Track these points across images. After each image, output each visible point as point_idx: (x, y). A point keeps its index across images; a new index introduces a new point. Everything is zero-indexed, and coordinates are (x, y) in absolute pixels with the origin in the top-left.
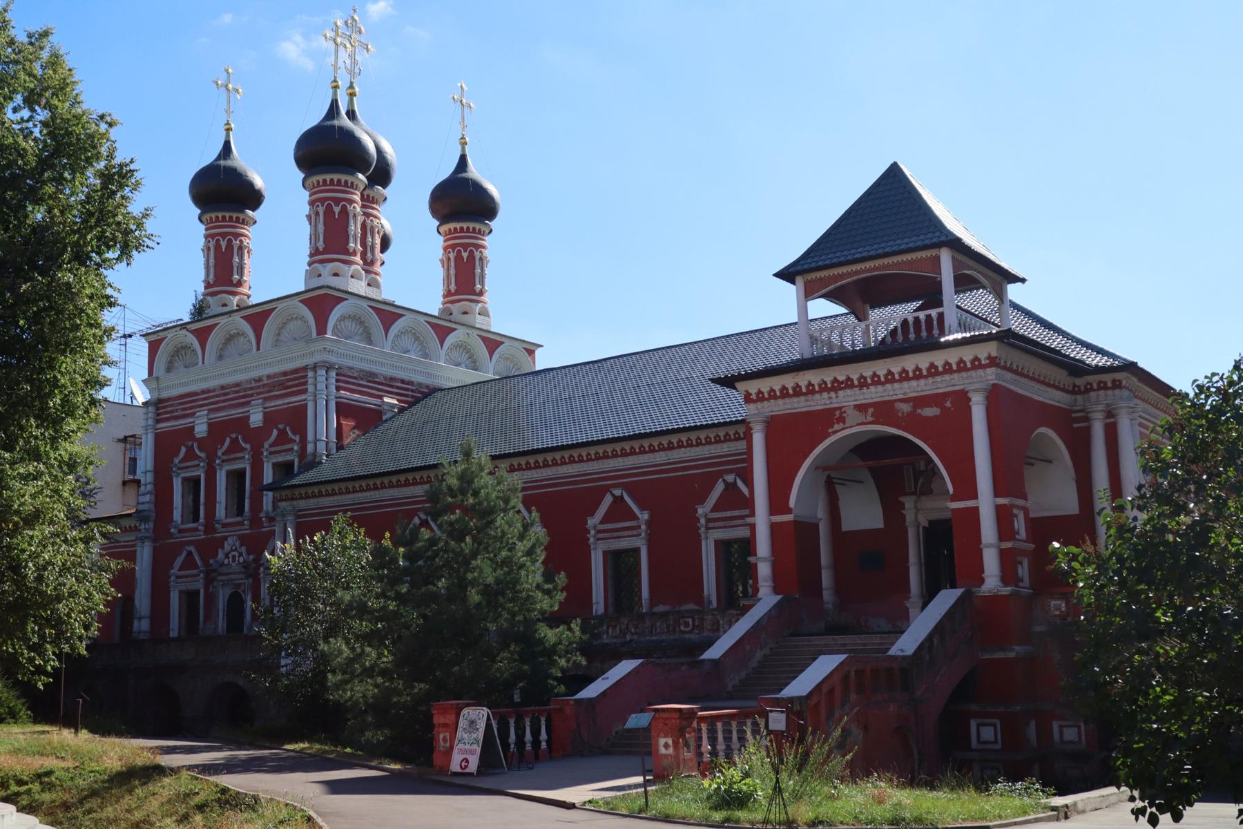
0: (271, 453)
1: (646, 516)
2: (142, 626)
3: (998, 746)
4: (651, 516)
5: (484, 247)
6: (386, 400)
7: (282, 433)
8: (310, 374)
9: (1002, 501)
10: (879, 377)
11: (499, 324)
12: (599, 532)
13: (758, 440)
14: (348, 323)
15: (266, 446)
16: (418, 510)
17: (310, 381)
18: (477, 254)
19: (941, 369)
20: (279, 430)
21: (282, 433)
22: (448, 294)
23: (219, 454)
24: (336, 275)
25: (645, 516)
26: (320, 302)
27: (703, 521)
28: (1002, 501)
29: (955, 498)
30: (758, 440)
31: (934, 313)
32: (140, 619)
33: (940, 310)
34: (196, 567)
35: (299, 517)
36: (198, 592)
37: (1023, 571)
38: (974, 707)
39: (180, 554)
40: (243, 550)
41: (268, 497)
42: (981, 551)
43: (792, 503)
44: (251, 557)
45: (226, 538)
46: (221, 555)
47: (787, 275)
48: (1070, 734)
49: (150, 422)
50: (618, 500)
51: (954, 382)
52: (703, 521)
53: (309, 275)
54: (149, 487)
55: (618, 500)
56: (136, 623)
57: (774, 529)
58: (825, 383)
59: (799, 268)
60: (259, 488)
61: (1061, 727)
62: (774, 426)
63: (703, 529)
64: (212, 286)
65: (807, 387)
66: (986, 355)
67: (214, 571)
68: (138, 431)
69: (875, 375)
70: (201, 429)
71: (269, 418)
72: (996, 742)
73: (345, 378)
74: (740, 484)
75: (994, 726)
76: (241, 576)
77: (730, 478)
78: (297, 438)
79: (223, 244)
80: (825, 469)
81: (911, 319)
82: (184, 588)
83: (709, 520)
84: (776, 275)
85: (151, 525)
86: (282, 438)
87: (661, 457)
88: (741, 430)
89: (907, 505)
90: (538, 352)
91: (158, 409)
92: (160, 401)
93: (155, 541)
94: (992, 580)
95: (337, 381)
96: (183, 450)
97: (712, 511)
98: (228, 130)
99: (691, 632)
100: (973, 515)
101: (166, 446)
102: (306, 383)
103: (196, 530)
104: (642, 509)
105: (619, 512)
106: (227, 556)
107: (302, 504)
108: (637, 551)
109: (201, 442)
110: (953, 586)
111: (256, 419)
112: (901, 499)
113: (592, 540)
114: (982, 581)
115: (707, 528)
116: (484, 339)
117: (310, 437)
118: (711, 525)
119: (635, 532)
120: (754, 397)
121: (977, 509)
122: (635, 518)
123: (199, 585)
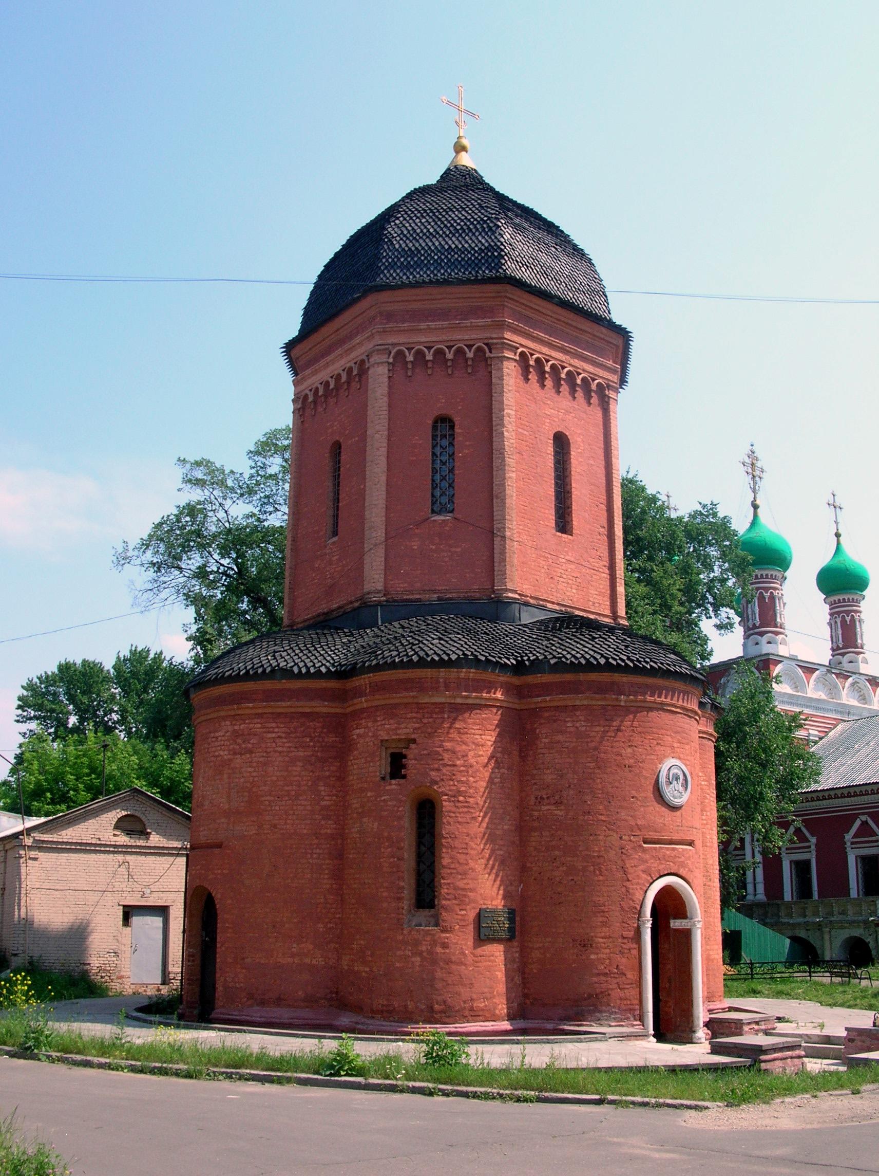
5: (860, 612)
16: (859, 814)
18: (856, 617)
22: (835, 650)
53: (745, 646)
116: (868, 680)
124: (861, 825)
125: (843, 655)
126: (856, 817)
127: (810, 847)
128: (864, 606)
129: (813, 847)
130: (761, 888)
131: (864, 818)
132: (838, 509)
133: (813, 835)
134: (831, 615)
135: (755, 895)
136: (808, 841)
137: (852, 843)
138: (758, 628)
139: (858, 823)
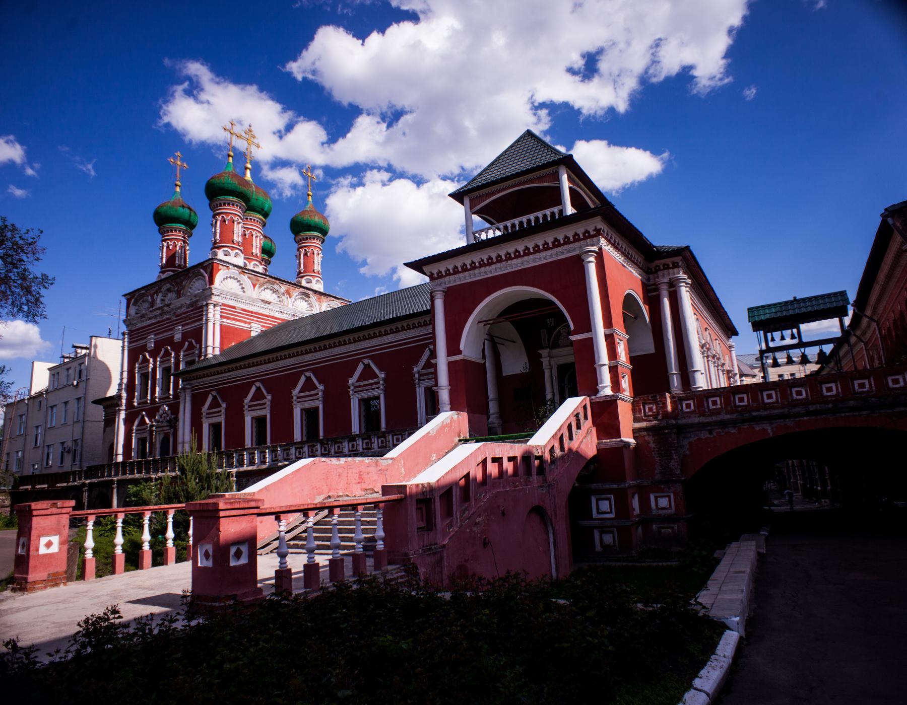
1: (383, 376)
3: (612, 516)
4: (386, 375)
7: (190, 343)
8: (205, 308)
9: (609, 331)
12: (356, 387)
19: (562, 242)
21: (190, 343)
25: (382, 375)
27: (417, 376)
29: (576, 332)
31: (556, 210)
33: (559, 207)
38: (594, 486)
39: (137, 417)
43: (462, 347)
48: (663, 502)
50: (367, 367)
52: (417, 376)
55: (367, 367)
57: (450, 364)
58: (482, 260)
61: (656, 498)
62: (450, 295)
65: (471, 265)
69: (517, 251)
71: (185, 336)
72: (611, 512)
73: (228, 311)
75: (609, 499)
78: (198, 346)
83: (420, 375)
84: (450, 195)
86: (191, 346)
87: (391, 338)
102: (202, 315)
104: (381, 370)
105: (368, 373)
108: (378, 398)
110: (576, 395)
111: (178, 337)
112: (540, 352)
114: (597, 391)
115: (420, 380)
118: (422, 378)
119: (377, 386)
120: (436, 275)
122: (376, 376)
123: (147, 435)
125: (302, 277)
126: (252, 383)
129: (223, 411)
133: (224, 401)
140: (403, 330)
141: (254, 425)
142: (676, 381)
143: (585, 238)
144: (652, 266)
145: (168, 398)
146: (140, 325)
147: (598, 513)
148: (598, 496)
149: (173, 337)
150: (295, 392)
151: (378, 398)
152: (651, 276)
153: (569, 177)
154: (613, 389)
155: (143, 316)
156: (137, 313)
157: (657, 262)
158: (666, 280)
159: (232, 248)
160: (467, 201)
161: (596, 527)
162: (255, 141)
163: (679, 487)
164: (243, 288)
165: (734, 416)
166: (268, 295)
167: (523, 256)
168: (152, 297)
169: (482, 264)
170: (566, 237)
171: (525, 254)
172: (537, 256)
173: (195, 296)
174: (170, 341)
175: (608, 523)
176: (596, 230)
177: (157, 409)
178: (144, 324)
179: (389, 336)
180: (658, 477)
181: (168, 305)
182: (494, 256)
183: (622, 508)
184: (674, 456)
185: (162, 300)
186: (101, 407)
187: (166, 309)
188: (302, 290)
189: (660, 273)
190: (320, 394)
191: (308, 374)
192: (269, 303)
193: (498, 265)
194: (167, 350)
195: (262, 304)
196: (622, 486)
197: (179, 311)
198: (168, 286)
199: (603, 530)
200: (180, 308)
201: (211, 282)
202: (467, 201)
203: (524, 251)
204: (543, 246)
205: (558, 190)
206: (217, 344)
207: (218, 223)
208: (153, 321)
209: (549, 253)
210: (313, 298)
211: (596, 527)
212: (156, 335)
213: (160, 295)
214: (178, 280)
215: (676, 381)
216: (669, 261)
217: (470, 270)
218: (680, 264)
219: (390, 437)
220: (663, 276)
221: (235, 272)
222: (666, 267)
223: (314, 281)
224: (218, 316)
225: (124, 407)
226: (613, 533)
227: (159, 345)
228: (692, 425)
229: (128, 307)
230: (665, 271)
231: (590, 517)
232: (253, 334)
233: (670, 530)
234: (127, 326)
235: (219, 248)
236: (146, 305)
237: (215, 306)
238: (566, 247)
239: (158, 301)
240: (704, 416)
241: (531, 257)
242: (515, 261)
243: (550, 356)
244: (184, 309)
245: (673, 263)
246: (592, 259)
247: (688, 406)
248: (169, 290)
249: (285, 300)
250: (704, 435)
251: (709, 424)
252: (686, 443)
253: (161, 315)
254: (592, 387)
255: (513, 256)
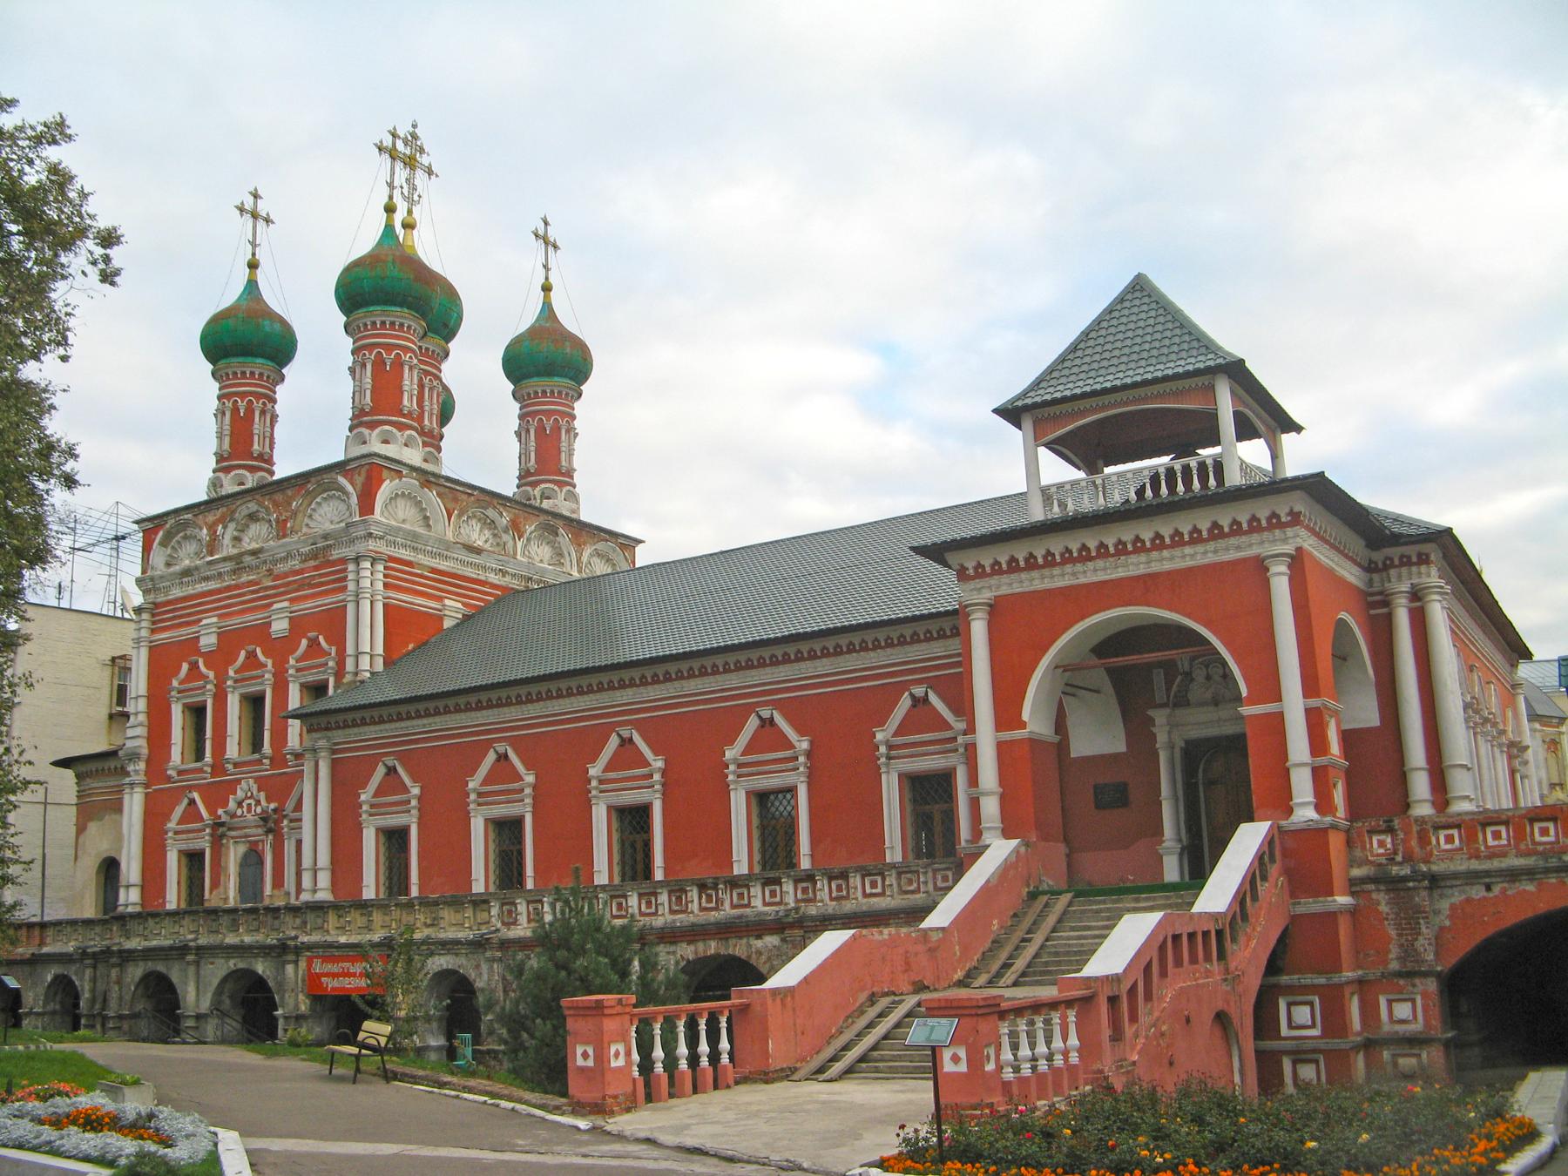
0: (298, 670)
1: (805, 745)
2: (130, 898)
3: (1316, 1032)
6: (447, 602)
7: (314, 643)
8: (351, 567)
9: (1314, 702)
10: (1143, 542)
11: (586, 516)
12: (740, 766)
13: (979, 629)
14: (401, 503)
15: (292, 662)
17: (351, 576)
18: (563, 423)
19: (1226, 530)
20: (309, 640)
21: (314, 643)
22: (524, 476)
23: (231, 673)
24: (386, 442)
26: (363, 474)
27: (883, 749)
28: (1314, 702)
29: (1252, 701)
30: (979, 629)
32: (128, 887)
34: (201, 819)
35: (334, 752)
36: (201, 854)
37: (1339, 796)
38: (1285, 979)
39: (178, 802)
40: (262, 794)
41: (294, 726)
42: (1287, 773)
43: (1025, 716)
44: (272, 806)
45: (239, 781)
46: (232, 805)
47: (1011, 413)
49: (144, 633)
51: (1252, 547)
52: (883, 749)
54: (142, 718)
56: (122, 892)
57: (1002, 748)
59: (1029, 401)
60: (282, 717)
61: (1390, 1002)
63: (883, 760)
64: (225, 460)
65: (1045, 557)
66: (1287, 510)
67: (222, 824)
68: (128, 650)
69: (1138, 539)
70: (208, 641)
72: (1313, 1026)
73: (398, 572)
74: (934, 699)
75: (1311, 1004)
76: (260, 831)
77: (919, 691)
78: (333, 650)
79: (242, 405)
80: (1066, 669)
81: (1178, 467)
82: (184, 847)
83: (890, 747)
84: (996, 411)
85: (142, 766)
87: (824, 666)
88: (947, 624)
89: (1157, 722)
90: (639, 549)
91: (153, 615)
92: (157, 605)
93: (147, 786)
94: (1305, 813)
95: (385, 576)
96: (185, 667)
97: (896, 734)
98: (253, 265)
99: (883, 894)
100: (1276, 723)
101: (162, 663)
103: (200, 770)
104: (801, 732)
105: (768, 736)
106: (240, 804)
107: (339, 736)
109: (208, 656)
111: (280, 626)
112: (1151, 713)
113: (731, 777)
115: (889, 758)
117: (350, 650)
119: (790, 765)
120: (971, 572)
121: (1279, 718)
122: (791, 746)
123: (204, 843)
124: (498, 760)
125: (534, 484)
126: (488, 744)
127: (409, 802)
128: (579, 408)
130: (324, 879)
131: (501, 747)
132: (550, 249)
134: (521, 417)
135: (315, 891)
136: (406, 790)
137: (480, 794)
138: (367, 414)
139: (491, 757)
140: (849, 651)
141: (492, 835)
142: (1420, 785)
143: (1271, 527)
144: (1378, 556)
145: (259, 762)
146: (177, 593)
147: (1290, 1026)
148: (1291, 999)
149: (269, 624)
150: (594, 771)
151: (792, 790)
152: (1376, 577)
153: (1232, 392)
154: (1318, 808)
155: (187, 572)
156: (168, 565)
157: (1389, 551)
158: (1405, 587)
159: (401, 427)
160: (1028, 423)
161: (1287, 1053)
162: (425, 160)
163: (1432, 985)
164: (426, 518)
165: (1529, 862)
166: (476, 534)
167: (1150, 550)
168: (212, 529)
169: (1068, 558)
170: (1235, 522)
171: (1154, 548)
172: (1177, 552)
173: (325, 537)
174: (261, 632)
175: (1309, 1045)
176: (1291, 513)
177: (232, 786)
178: (190, 591)
179: (817, 663)
180: (1394, 966)
181: (254, 553)
182: (1092, 545)
183: (1333, 1020)
184: (1424, 930)
185: (237, 539)
186: (69, 774)
187: (248, 559)
188: (542, 518)
189: (1393, 572)
190: (657, 777)
191: (625, 733)
192: (478, 551)
193: (1100, 563)
194: (251, 655)
195: (464, 552)
196: (1336, 980)
197: (282, 568)
198: (253, 507)
199: (1300, 1056)
200: (285, 559)
201: (367, 506)
202: (1028, 423)
203: (1153, 541)
204: (1191, 533)
205: (1212, 417)
206: (380, 649)
207: (369, 367)
208: (213, 585)
209: (1200, 548)
210: (564, 538)
211: (1287, 1053)
212: (220, 616)
213: (232, 526)
214: (279, 497)
215: (1420, 785)
216: (1412, 551)
217: (1043, 567)
218: (1432, 558)
219: (858, 879)
220: (1400, 577)
221: (412, 482)
222: (1406, 562)
223: (561, 496)
224: (380, 586)
225: (142, 778)
226: (1317, 1062)
227: (229, 642)
228: (1455, 875)
229: (147, 549)
230: (1404, 570)
231: (1278, 1037)
232: (448, 624)
233: (1413, 1061)
234: (146, 592)
235: (372, 426)
236: (191, 548)
237: (374, 561)
238: (1233, 541)
239: (227, 540)
240: (1477, 857)
241: (1165, 553)
242: (1133, 559)
243: (1172, 726)
244: (295, 563)
245: (1419, 555)
246: (1283, 569)
247: (1449, 839)
248: (253, 517)
249: (511, 543)
250: (1477, 892)
251: (1487, 873)
252: (1444, 905)
253: (234, 572)
254: (1283, 802)
255: (1130, 547)
